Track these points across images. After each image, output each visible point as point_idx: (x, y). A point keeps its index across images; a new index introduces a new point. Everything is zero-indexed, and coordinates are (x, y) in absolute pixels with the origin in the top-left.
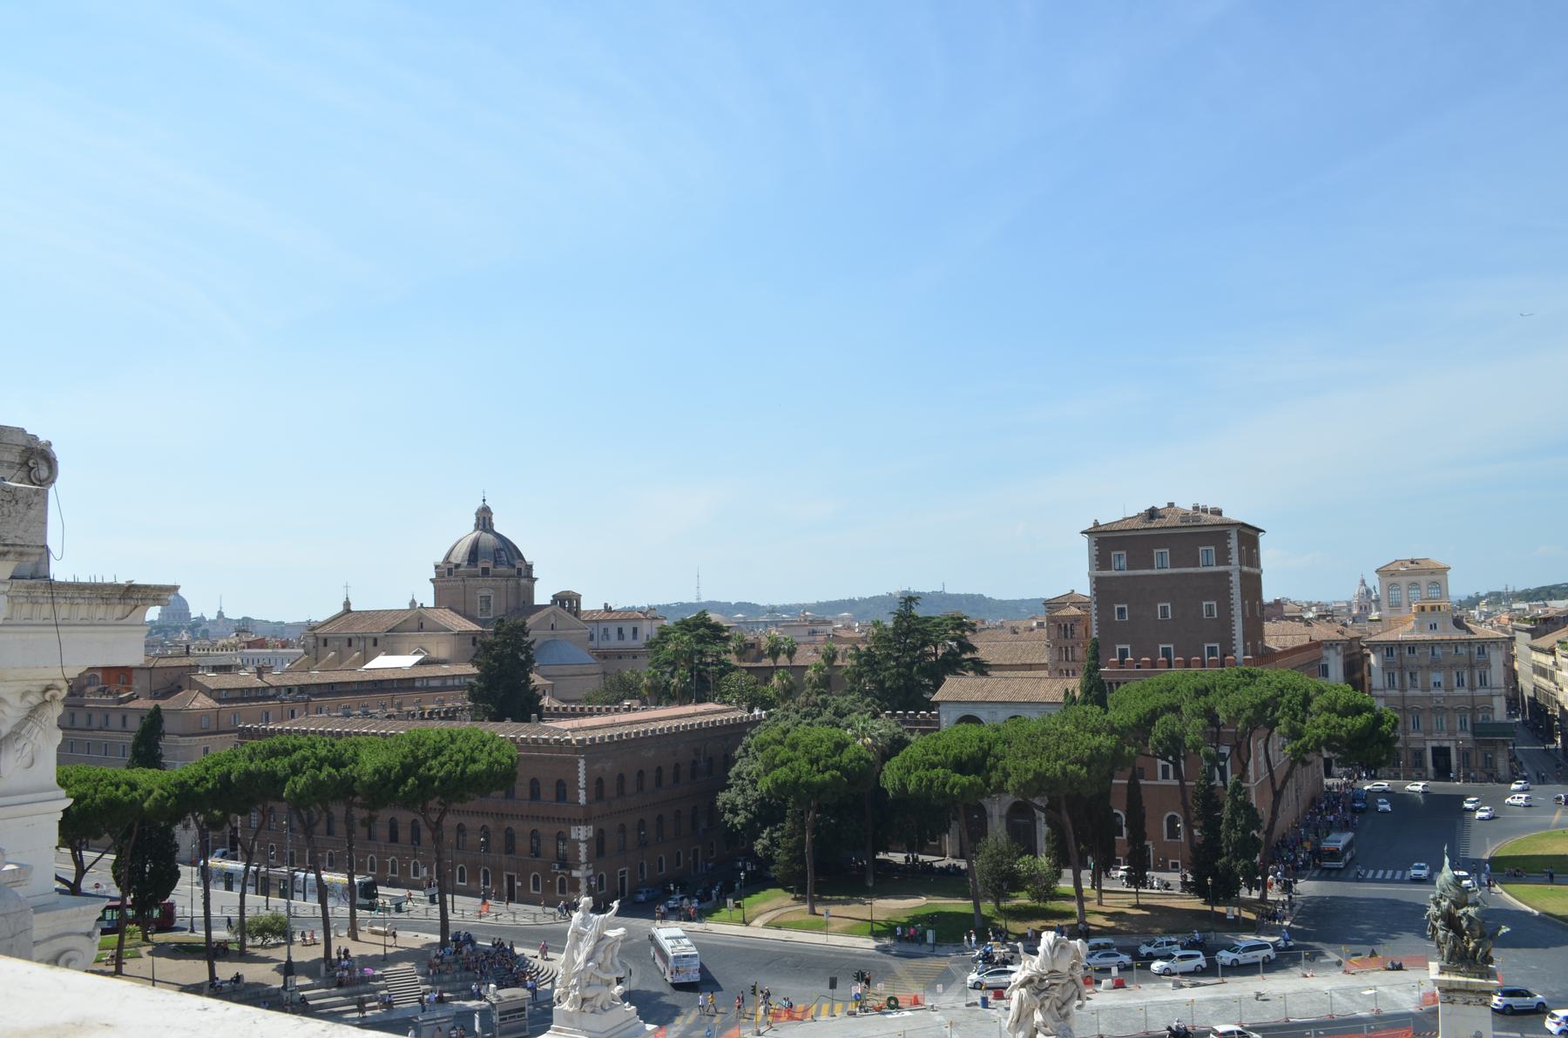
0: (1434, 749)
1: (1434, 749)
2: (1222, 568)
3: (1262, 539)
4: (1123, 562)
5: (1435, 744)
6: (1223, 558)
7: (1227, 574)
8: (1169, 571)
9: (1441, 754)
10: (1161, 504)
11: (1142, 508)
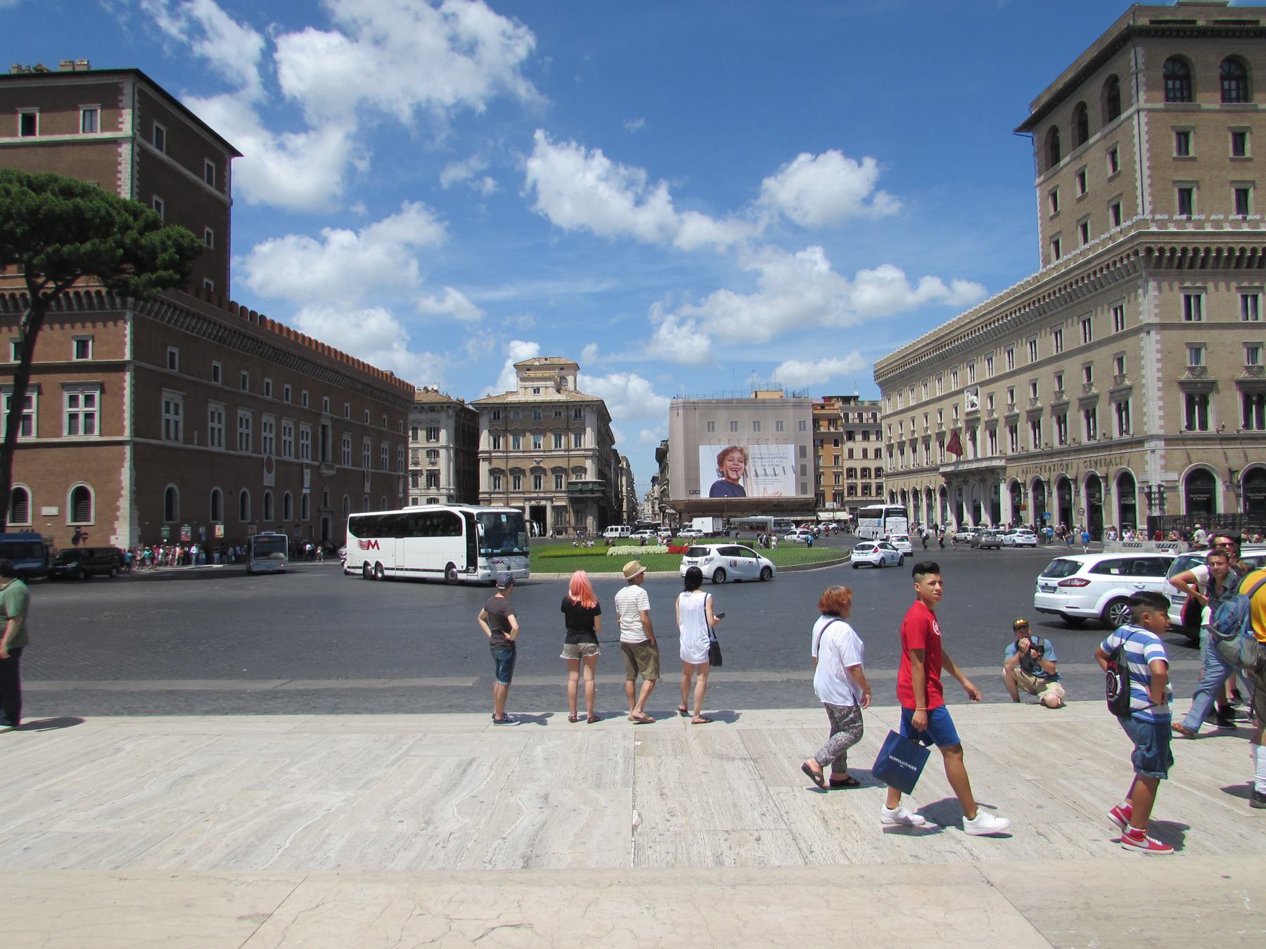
0: (532, 508)
5: (533, 503)
8: (37, 138)
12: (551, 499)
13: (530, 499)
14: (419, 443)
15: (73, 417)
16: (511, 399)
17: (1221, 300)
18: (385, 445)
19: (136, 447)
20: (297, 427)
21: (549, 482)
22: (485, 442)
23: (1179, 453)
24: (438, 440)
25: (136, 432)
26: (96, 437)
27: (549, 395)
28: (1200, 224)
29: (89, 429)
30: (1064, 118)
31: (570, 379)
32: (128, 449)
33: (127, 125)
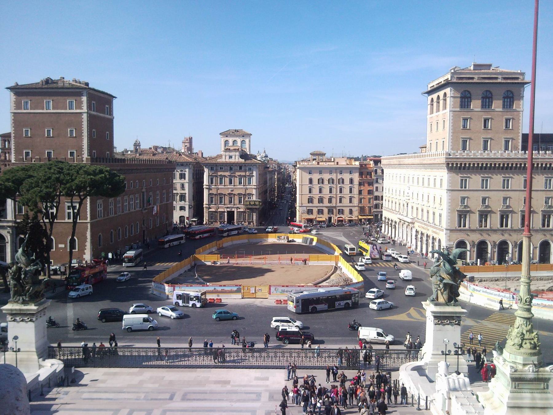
1: (228, 212)
3: (115, 101)
5: (228, 210)
9: (231, 214)
10: (55, 77)
11: (44, 77)
12: (237, 208)
13: (228, 208)
14: (177, 181)
15: (69, 213)
16: (219, 161)
17: (475, 181)
18: (164, 191)
19: (91, 224)
20: (135, 196)
22: (206, 181)
24: (185, 179)
25: (91, 219)
27: (236, 159)
31: (247, 141)
32: (89, 225)
33: (85, 109)
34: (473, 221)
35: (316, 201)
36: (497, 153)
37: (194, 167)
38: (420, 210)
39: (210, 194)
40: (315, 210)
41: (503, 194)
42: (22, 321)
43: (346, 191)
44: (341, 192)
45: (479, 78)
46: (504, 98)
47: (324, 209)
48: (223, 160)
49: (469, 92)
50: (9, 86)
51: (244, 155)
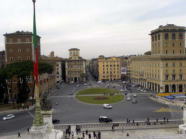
2: (30, 43)
3: (41, 39)
4: (12, 41)
5: (75, 77)
6: (31, 41)
7: (31, 44)
8: (21, 43)
9: (76, 79)
17: (170, 63)
21: (77, 73)
22: (66, 67)
23: (164, 82)
26: (31, 82)
27: (77, 59)
28: (168, 55)
29: (30, 81)
30: (154, 36)
34: (170, 77)
35: (106, 73)
36: (177, 54)
37: (62, 62)
38: (149, 74)
39: (68, 72)
40: (106, 76)
41: (180, 68)
42: (46, 117)
43: (116, 68)
44: (114, 69)
45: (171, 29)
46: (179, 36)
47: (109, 75)
48: (72, 59)
49: (167, 34)
50: (4, 34)
51: (79, 57)
